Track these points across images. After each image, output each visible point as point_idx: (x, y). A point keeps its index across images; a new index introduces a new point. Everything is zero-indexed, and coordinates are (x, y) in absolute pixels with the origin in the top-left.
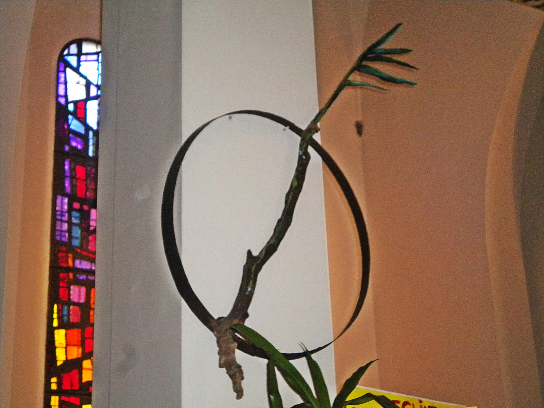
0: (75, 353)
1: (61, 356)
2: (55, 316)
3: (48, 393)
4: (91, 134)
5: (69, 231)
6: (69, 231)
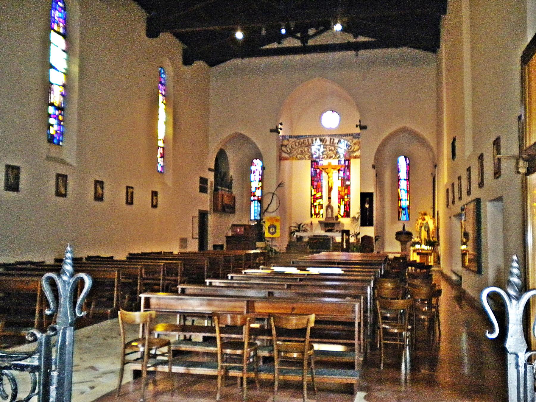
0: (315, 193)
1: (313, 194)
3: (311, 199)
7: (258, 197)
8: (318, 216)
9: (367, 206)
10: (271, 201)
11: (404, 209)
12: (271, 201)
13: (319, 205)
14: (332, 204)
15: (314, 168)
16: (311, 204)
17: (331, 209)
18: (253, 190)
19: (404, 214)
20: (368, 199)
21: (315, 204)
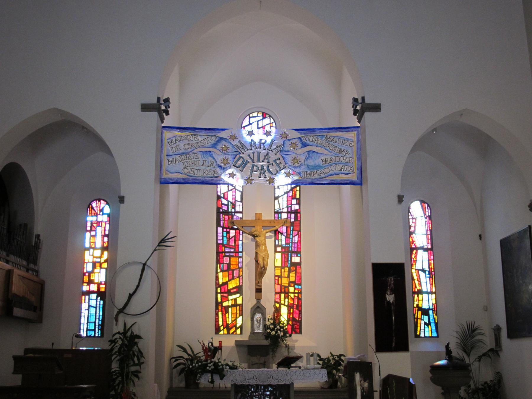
1: (221, 282)
2: (219, 268)
3: (217, 293)
4: (230, 203)
5: (223, 239)
6: (223, 239)
7: (99, 284)
8: (232, 331)
9: (390, 298)
10: (138, 286)
11: (425, 312)
12: (138, 286)
13: (235, 305)
14: (262, 302)
15: (223, 228)
16: (217, 303)
17: (262, 314)
18: (89, 267)
19: (425, 323)
20: (391, 280)
21: (225, 304)
